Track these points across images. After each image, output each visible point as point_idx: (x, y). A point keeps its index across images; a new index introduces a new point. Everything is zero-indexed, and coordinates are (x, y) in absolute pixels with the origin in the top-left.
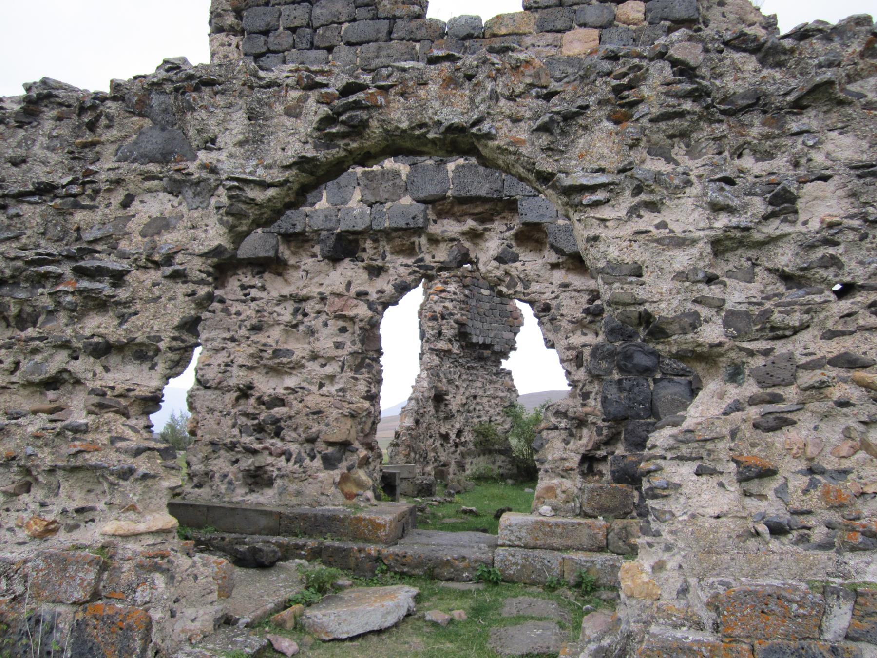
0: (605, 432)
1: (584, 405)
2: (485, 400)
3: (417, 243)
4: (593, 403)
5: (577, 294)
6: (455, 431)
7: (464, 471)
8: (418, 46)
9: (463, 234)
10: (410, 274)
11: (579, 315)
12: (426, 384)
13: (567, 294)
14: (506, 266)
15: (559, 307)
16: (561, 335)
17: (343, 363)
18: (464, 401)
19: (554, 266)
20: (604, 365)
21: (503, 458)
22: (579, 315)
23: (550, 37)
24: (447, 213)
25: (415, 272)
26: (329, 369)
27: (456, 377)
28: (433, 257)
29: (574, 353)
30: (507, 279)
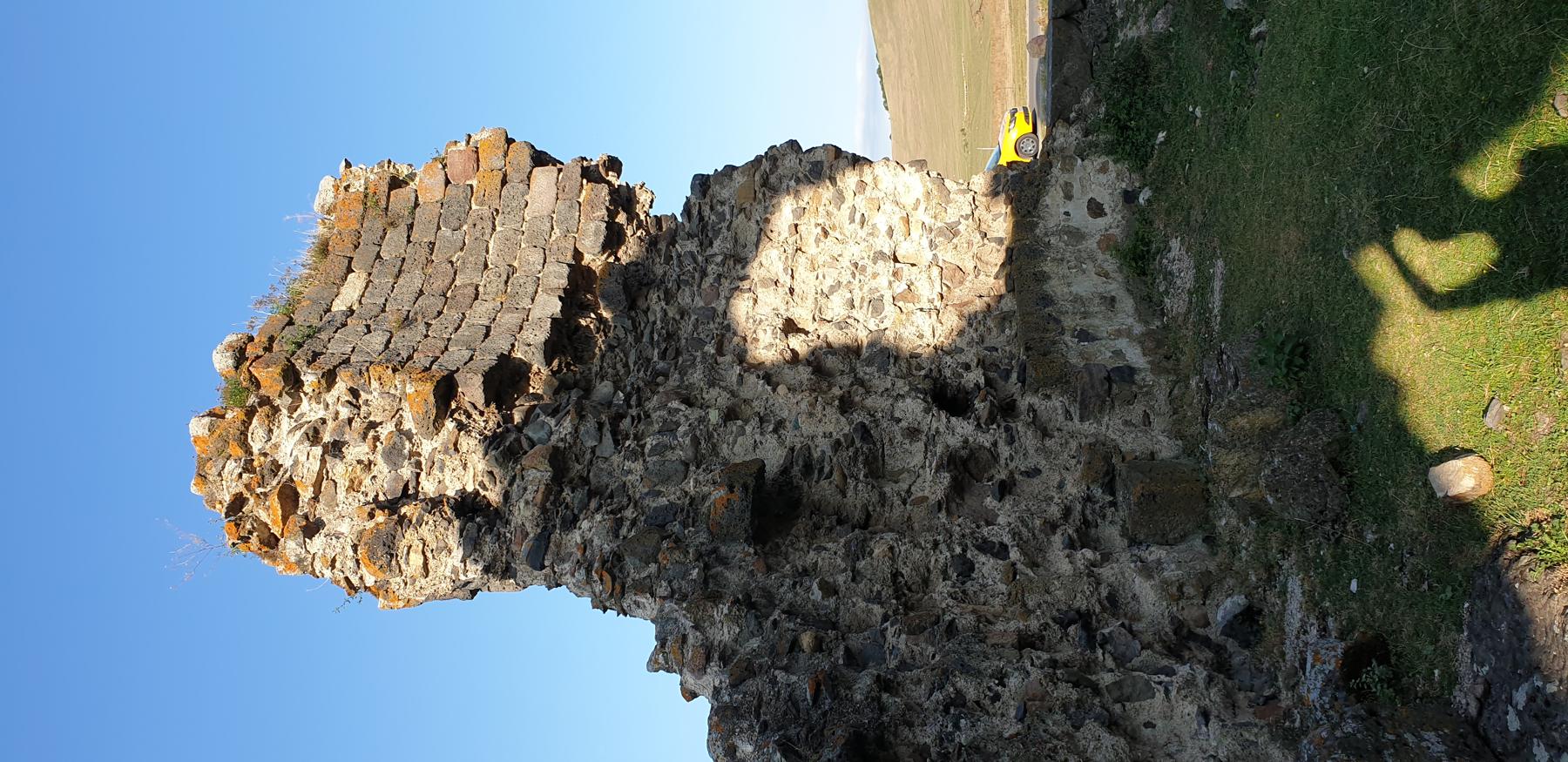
2: (806, 281)
6: (938, 421)
7: (1128, 373)
21: (1053, 199)
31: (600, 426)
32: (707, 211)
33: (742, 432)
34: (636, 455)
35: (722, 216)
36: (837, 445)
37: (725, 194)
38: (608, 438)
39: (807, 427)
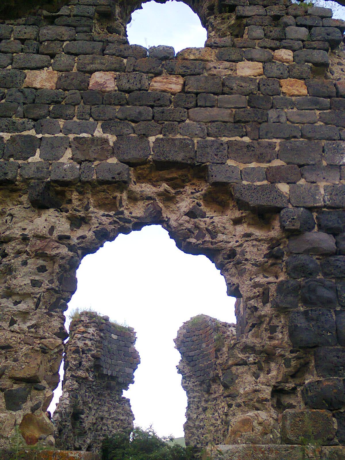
0: (293, 363)
1: (271, 338)
2: (110, 422)
3: (119, 198)
4: (280, 336)
5: (257, 243)
8: (125, 61)
9: (159, 194)
10: (110, 223)
11: (261, 259)
12: (67, 402)
13: (250, 243)
14: (196, 220)
15: (243, 253)
16: (246, 276)
17: (39, 299)
18: (94, 421)
19: (237, 222)
20: (290, 298)
22: (261, 259)
23: (227, 64)
24: (144, 178)
25: (115, 222)
26: (22, 306)
27: (90, 400)
28: (131, 213)
29: (261, 290)
30: (196, 232)
31: (90, 385)
32: (123, 402)
33: (87, 410)
34: (86, 392)
35: (122, 404)
36: (84, 427)
37: (126, 405)
38: (88, 386)
39: (87, 422)
